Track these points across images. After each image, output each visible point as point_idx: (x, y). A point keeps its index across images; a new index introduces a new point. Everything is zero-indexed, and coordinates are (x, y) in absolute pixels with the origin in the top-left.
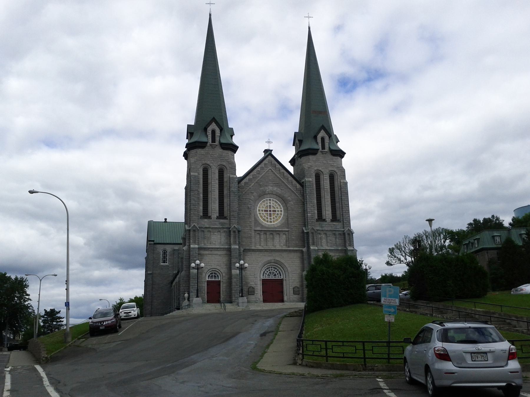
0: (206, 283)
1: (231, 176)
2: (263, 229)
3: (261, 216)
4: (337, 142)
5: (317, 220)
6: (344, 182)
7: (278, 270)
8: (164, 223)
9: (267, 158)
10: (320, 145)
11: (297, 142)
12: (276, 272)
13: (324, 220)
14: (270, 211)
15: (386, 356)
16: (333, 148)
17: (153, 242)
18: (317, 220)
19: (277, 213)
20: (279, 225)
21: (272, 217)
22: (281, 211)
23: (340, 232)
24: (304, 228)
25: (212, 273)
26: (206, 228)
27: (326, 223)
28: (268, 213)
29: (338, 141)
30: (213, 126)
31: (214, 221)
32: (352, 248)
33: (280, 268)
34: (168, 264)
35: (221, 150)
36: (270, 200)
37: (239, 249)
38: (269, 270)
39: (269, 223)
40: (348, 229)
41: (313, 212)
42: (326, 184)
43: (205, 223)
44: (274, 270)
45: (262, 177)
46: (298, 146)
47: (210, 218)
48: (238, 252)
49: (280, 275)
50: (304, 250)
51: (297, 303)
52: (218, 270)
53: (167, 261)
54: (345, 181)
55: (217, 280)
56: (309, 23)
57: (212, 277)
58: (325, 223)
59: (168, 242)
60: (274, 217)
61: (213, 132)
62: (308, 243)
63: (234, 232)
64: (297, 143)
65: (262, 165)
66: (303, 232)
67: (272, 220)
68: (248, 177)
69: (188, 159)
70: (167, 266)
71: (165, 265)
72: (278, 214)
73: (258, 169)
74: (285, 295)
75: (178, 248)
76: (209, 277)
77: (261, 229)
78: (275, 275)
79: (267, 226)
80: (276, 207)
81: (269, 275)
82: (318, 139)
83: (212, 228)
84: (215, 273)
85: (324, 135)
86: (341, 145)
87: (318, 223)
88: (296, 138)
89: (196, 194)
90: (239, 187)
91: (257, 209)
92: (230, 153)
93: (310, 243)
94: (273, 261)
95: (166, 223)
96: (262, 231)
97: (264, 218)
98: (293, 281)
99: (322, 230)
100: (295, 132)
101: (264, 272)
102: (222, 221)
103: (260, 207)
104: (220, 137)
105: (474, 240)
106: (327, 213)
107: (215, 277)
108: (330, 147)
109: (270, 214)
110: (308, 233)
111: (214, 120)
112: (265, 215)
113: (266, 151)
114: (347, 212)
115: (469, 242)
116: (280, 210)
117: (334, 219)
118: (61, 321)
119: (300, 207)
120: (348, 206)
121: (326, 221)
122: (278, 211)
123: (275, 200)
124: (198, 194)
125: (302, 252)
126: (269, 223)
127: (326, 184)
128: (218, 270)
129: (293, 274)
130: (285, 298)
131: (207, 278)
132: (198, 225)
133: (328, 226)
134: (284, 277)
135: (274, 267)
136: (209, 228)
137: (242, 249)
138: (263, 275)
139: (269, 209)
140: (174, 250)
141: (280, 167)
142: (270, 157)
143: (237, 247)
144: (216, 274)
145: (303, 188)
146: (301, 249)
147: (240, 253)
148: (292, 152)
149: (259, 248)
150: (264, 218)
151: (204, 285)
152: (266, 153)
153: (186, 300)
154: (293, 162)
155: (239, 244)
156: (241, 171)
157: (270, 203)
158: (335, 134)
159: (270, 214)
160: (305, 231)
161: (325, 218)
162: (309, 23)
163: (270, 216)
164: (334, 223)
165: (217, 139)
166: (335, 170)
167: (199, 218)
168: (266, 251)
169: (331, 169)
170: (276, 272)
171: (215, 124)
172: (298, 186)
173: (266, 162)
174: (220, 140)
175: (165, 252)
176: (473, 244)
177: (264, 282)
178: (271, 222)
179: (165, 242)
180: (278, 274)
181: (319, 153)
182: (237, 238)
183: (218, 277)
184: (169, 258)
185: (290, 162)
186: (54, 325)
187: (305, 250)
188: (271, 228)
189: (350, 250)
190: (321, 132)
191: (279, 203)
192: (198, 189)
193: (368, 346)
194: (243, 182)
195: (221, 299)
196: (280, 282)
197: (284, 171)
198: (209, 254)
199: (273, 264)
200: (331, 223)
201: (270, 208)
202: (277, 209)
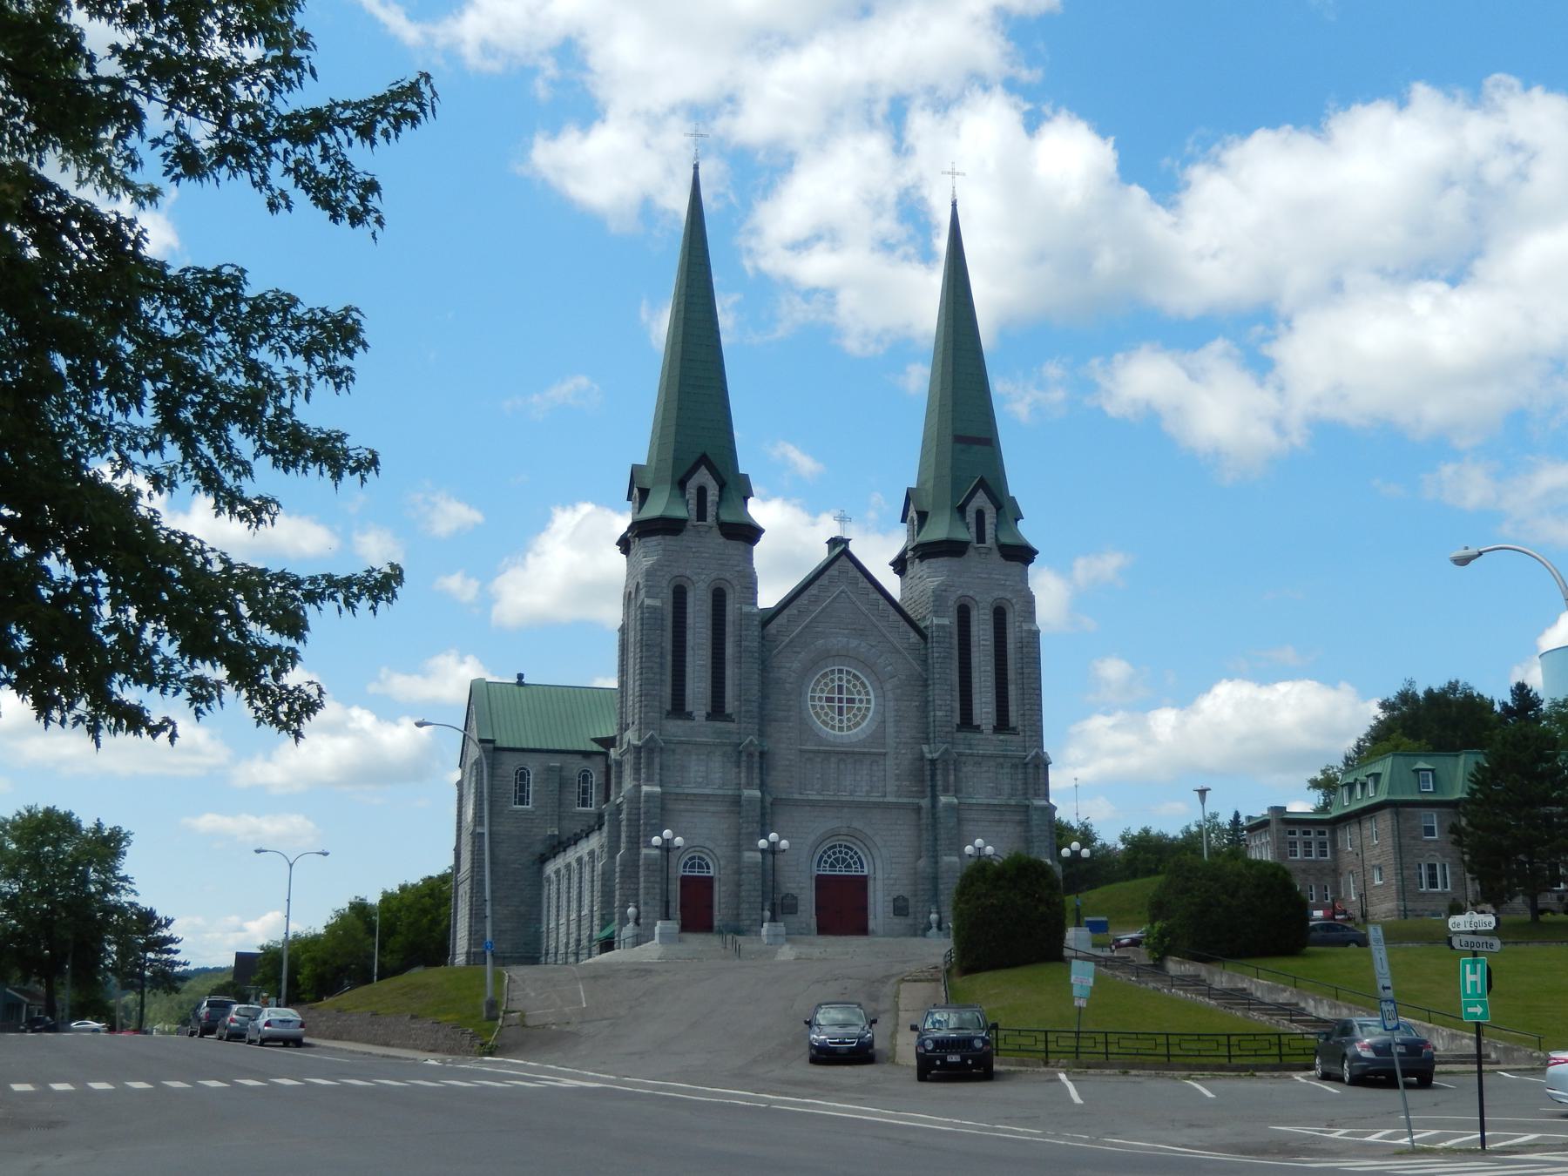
0: (679, 883)
1: (746, 609)
2: (822, 748)
3: (817, 714)
4: (1017, 520)
5: (960, 728)
6: (1030, 631)
7: (856, 853)
8: (516, 688)
9: (838, 563)
10: (973, 529)
11: (912, 514)
12: (852, 857)
13: (978, 729)
14: (840, 700)
15: (1074, 1049)
16: (1006, 539)
17: (491, 746)
18: (960, 728)
19: (857, 705)
20: (862, 736)
21: (845, 717)
22: (868, 701)
23: (1014, 761)
24: (925, 748)
25: (694, 858)
26: (681, 743)
27: (983, 736)
28: (834, 707)
29: (1018, 516)
30: (703, 477)
31: (699, 724)
32: (1043, 803)
33: (861, 849)
34: (533, 809)
35: (722, 540)
36: (840, 671)
37: (762, 800)
38: (834, 853)
39: (837, 732)
40: (1037, 753)
41: (948, 708)
42: (981, 632)
43: (675, 727)
44: (846, 854)
45: (822, 611)
46: (916, 527)
47: (689, 716)
48: (759, 804)
49: (862, 867)
50: (923, 806)
51: (903, 939)
52: (707, 851)
53: (528, 798)
54: (1034, 628)
55: (705, 874)
56: (954, 191)
57: (693, 866)
58: (979, 736)
59: (532, 746)
60: (850, 715)
61: (702, 492)
62: (933, 787)
63: (750, 755)
64: (912, 518)
65: (824, 580)
66: (922, 757)
67: (845, 725)
68: (786, 612)
69: (632, 552)
70: (527, 811)
71: (522, 810)
72: (859, 709)
73: (813, 590)
74: (871, 917)
75: (558, 765)
76: (685, 867)
77: (816, 748)
78: (849, 866)
79: (838, 740)
80: (855, 691)
81: (832, 865)
82: (967, 514)
83: (696, 744)
84: (700, 858)
85: (983, 504)
86: (1028, 531)
87: (961, 735)
88: (912, 505)
89: (657, 654)
90: (763, 638)
91: (807, 694)
92: (740, 545)
93: (940, 788)
94: (844, 831)
95: (522, 688)
96: (819, 752)
97: (823, 717)
98: (892, 882)
99: (971, 755)
100: (908, 489)
101: (821, 857)
102: (719, 724)
103: (814, 691)
104: (719, 504)
105: (1367, 776)
106: (984, 710)
107: (700, 867)
108: (999, 536)
109: (840, 709)
110: (933, 761)
111: (704, 460)
112: (827, 709)
113: (834, 542)
114: (1036, 707)
115: (1356, 780)
116: (864, 698)
117: (1002, 725)
118: (169, 951)
119: (916, 693)
120: (1037, 692)
121: (982, 732)
122: (861, 701)
123: (854, 671)
124: (662, 656)
125: (918, 809)
126: (837, 732)
127: (981, 632)
128: (707, 851)
129: (893, 866)
130: (872, 925)
131: (682, 869)
132: (660, 734)
133: (987, 742)
134: (872, 872)
135: (848, 844)
136: (688, 743)
137: (769, 799)
138: (819, 866)
139: (837, 704)
140: (551, 769)
141: (869, 585)
142: (844, 558)
143: (758, 793)
144: (703, 860)
145: (926, 643)
146: (917, 801)
147: (763, 808)
148: (898, 541)
149: (811, 797)
150: (823, 717)
151: (722, 901)
152: (834, 548)
153: (631, 925)
154: (900, 565)
155: (762, 786)
156: (768, 598)
157: (840, 679)
158: (1011, 495)
159: (840, 709)
160: (929, 756)
161: (978, 723)
162: (954, 191)
163: (840, 714)
164: (1001, 737)
165: (711, 510)
166: (1009, 596)
167: (664, 716)
168: (827, 804)
169: (998, 594)
170: (852, 857)
171: (706, 472)
172: (914, 637)
173: (833, 571)
174: (717, 514)
175: (522, 775)
176: (1364, 785)
177: (822, 883)
178: (841, 729)
179: (525, 746)
180: (855, 863)
181: (971, 552)
182: (756, 770)
183: (708, 868)
184: (535, 792)
185: (892, 564)
186: (150, 960)
187: (925, 803)
188: (843, 745)
189: (1037, 808)
190: (978, 495)
191: (863, 679)
192: (661, 643)
193: (1051, 1037)
194: (773, 628)
195: (716, 923)
196: (861, 883)
197: (877, 595)
198: (687, 811)
199: (845, 838)
200: (995, 737)
201: (840, 692)
202: (857, 697)
